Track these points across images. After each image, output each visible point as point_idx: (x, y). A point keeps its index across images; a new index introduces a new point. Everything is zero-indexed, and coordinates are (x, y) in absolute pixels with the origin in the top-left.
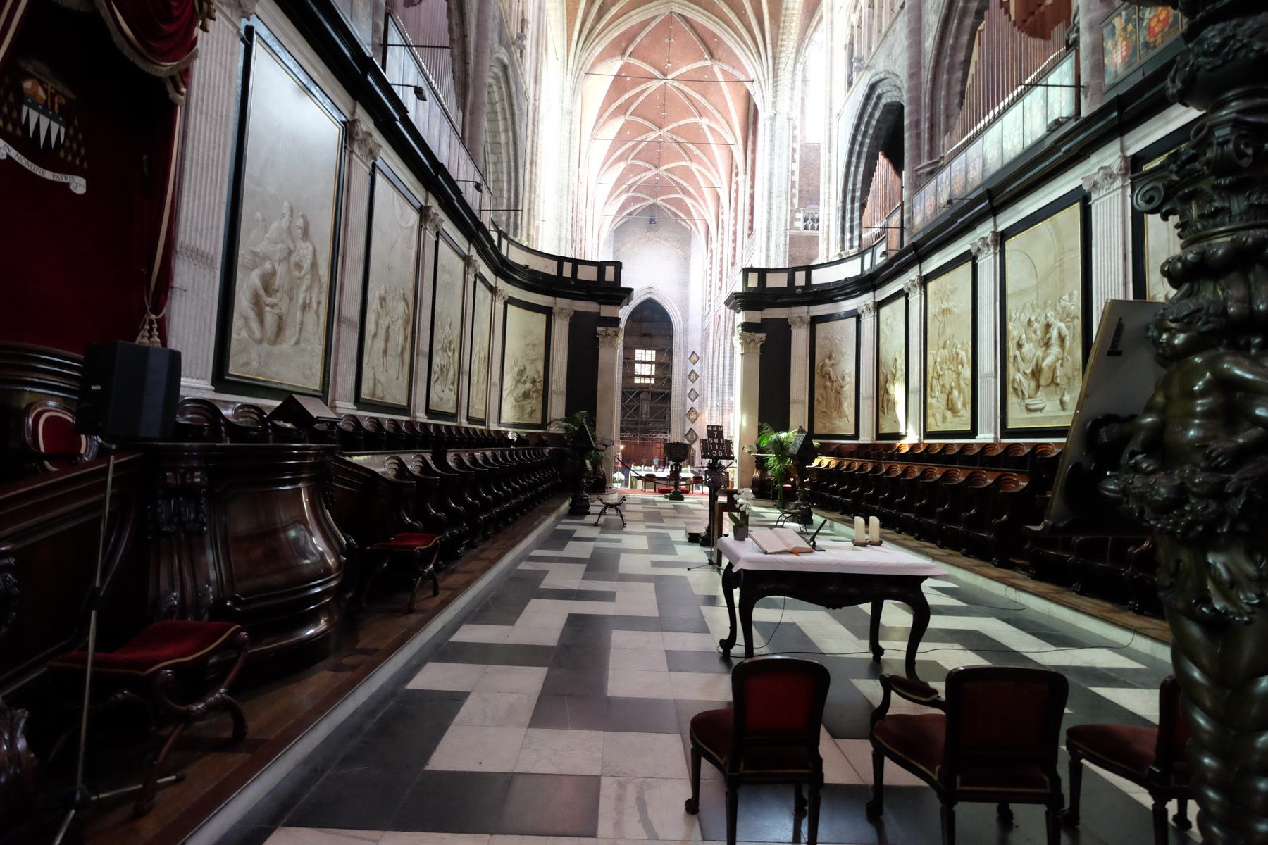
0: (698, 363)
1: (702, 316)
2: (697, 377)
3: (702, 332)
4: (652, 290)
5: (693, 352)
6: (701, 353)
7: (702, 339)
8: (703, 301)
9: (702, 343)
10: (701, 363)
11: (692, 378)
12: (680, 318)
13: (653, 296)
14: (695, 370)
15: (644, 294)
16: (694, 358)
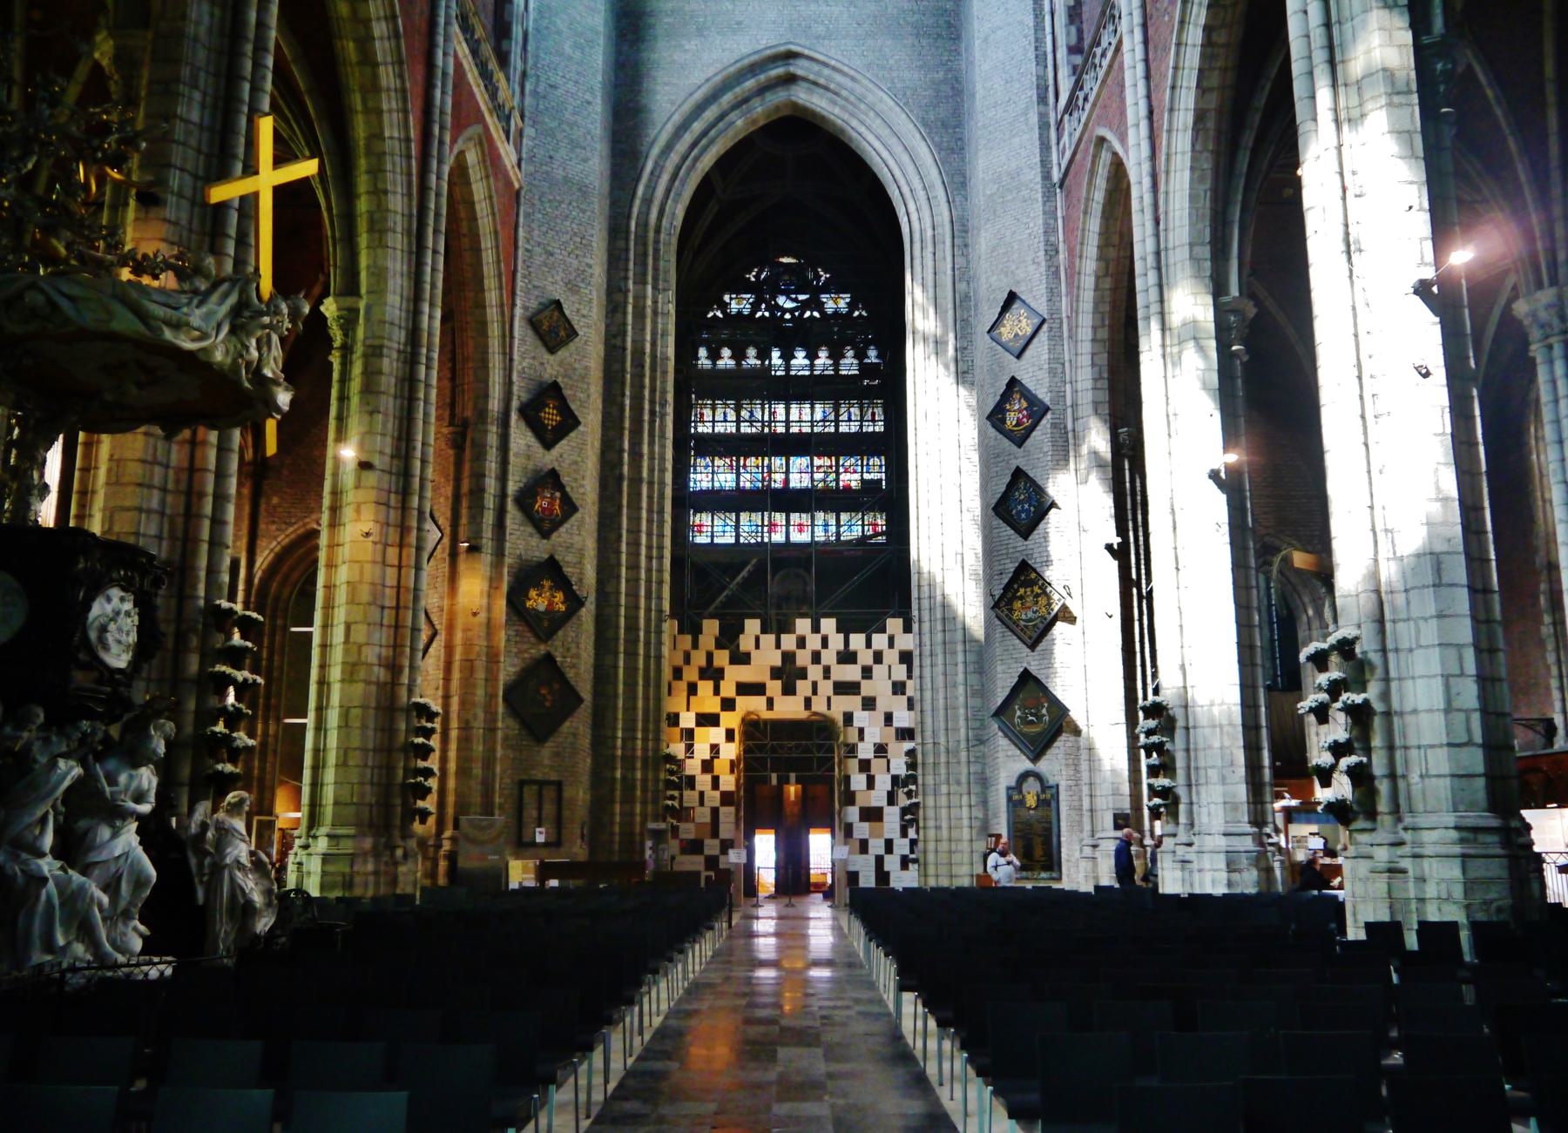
0: (1040, 346)
1: (1044, 126)
2: (1037, 411)
3: (1049, 195)
4: (799, 68)
5: (1012, 298)
6: (1053, 294)
7: (1049, 230)
8: (1040, 59)
9: (1051, 251)
10: (1055, 338)
11: (1011, 419)
12: (933, 174)
13: (802, 95)
14: (1027, 380)
15: (762, 91)
16: (1018, 324)
